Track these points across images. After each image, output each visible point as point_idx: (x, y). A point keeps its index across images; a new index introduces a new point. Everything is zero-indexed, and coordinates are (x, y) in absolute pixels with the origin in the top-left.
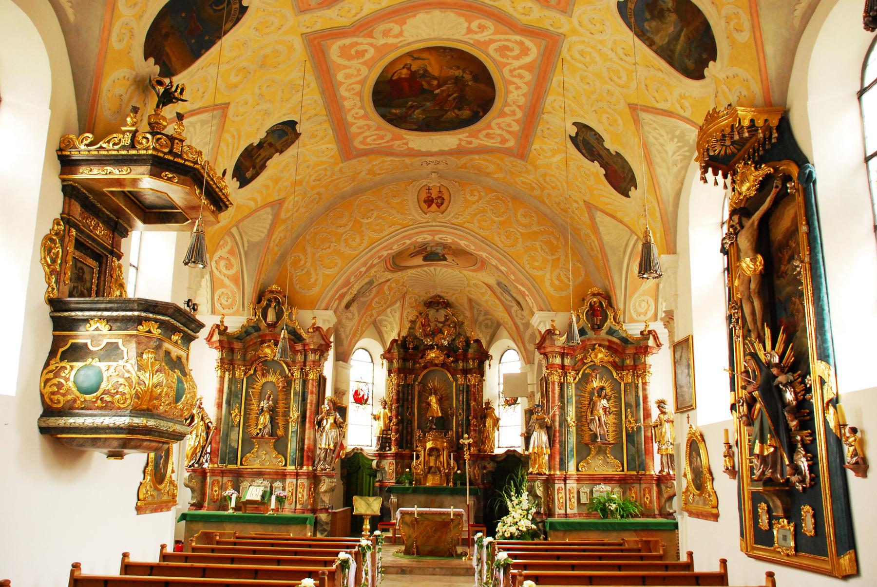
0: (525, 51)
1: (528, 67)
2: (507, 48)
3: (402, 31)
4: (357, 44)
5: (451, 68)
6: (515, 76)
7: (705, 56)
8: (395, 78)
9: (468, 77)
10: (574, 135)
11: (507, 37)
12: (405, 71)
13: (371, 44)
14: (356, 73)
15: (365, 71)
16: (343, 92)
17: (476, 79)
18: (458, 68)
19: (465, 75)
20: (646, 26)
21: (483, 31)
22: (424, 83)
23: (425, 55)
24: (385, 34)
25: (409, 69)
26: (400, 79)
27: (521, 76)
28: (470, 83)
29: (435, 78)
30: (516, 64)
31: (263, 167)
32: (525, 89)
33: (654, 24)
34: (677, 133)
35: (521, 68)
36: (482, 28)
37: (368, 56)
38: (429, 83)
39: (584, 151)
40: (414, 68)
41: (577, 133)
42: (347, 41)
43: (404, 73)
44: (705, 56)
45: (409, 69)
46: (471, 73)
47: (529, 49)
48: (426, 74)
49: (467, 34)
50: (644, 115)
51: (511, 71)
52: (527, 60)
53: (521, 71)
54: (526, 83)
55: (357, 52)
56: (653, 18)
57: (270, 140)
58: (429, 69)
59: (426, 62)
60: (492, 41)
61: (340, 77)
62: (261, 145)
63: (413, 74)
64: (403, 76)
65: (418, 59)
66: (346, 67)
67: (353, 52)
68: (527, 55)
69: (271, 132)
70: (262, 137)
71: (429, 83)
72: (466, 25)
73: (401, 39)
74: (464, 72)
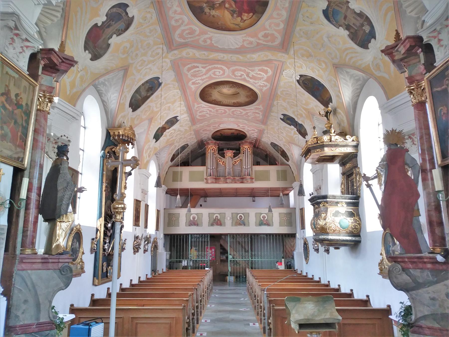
0: (181, 36)
1: (175, 28)
2: (189, 33)
3: (243, 42)
4: (266, 41)
5: (217, 16)
6: (180, 19)
7: (134, 107)
8: (251, 14)
9: (207, 10)
10: (128, 10)
11: (192, 39)
12: (245, 18)
13: (260, 39)
14: (273, 25)
15: (267, 25)
16: (284, 14)
17: (201, 9)
18: (213, 16)
19: (208, 11)
20: (148, 84)
21: (204, 39)
22: (234, 6)
23: (232, 26)
24: (251, 43)
25: (242, 19)
26: (248, 13)
27: (177, 21)
28: (205, 5)
29: (227, 8)
30: (182, 28)
31: (361, 15)
32: (171, 13)
33: (147, 87)
34: (106, 83)
35: (179, 26)
36: (205, 41)
37: (262, 33)
38: (231, 6)
39: (114, 10)
40: (239, 19)
41: (127, 14)
42: (270, 44)
43: (245, 16)
44: (134, 107)
45: (242, 19)
46: (205, 14)
47: (179, 37)
48: (233, 13)
49: (211, 37)
50: (122, 73)
51: (183, 22)
52: (178, 32)
53: (178, 24)
54: (173, 18)
55: (267, 37)
56: (149, 88)
57: (342, 21)
58: (230, 16)
59: (232, 22)
60: (198, 35)
61: (282, 26)
62: (348, 28)
63: (240, 15)
64: (246, 14)
65: (236, 25)
66: (276, 31)
67: (269, 38)
68: (179, 34)
69: (338, 25)
70: (343, 29)
71: (231, 6)
72: (213, 42)
73: (244, 38)
74: (209, 13)
